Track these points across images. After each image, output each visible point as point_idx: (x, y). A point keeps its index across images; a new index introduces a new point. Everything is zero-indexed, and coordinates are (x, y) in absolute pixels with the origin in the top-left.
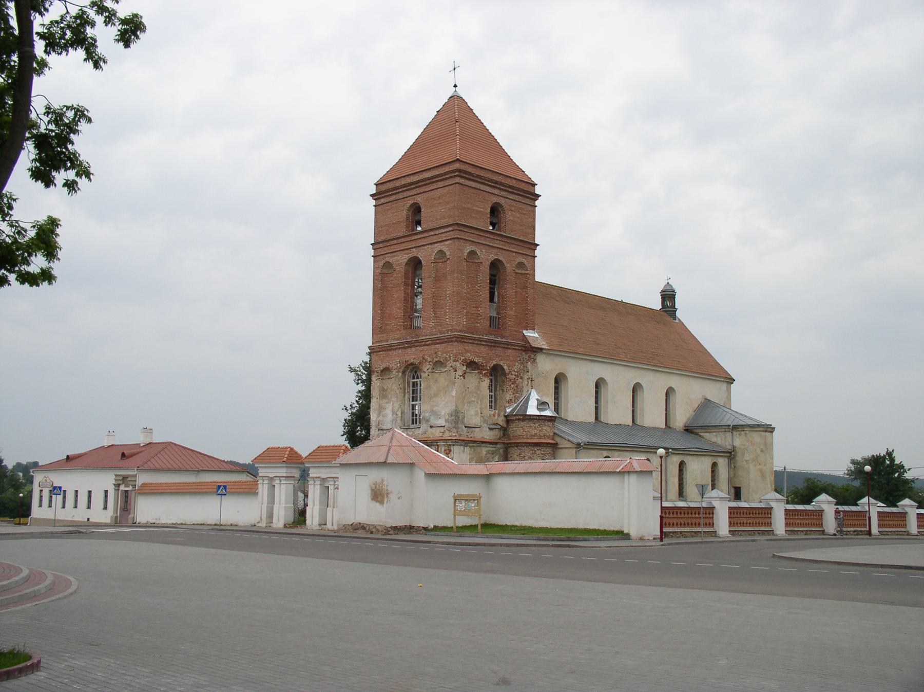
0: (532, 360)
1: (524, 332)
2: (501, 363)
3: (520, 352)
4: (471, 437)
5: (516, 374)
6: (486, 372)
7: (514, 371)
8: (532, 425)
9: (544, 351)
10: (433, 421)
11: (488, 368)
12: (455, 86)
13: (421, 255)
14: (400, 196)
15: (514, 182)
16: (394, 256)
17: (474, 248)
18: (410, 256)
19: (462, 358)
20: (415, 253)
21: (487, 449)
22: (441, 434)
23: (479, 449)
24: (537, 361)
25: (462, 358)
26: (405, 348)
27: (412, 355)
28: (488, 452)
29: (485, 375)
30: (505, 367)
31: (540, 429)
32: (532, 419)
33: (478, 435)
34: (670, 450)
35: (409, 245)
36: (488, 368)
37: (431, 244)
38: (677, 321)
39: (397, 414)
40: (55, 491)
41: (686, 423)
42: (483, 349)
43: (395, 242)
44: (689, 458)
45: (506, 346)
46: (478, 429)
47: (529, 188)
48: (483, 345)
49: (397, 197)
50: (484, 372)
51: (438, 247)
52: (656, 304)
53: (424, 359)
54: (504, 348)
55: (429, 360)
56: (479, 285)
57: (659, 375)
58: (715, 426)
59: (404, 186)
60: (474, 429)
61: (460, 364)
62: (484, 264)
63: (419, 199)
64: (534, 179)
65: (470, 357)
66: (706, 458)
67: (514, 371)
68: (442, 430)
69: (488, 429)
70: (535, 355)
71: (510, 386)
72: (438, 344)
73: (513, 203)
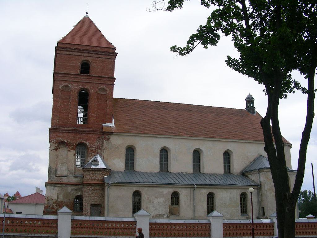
0: (107, 139)
1: (103, 124)
2: (85, 142)
3: (100, 135)
4: (60, 182)
5: (96, 147)
6: (73, 147)
7: (95, 146)
8: (89, 173)
9: (114, 134)
11: (75, 145)
15: (99, 48)
17: (67, 84)
19: (55, 140)
21: (72, 188)
23: (66, 188)
24: (111, 139)
25: (55, 140)
28: (72, 190)
29: (72, 149)
30: (88, 144)
31: (92, 176)
32: (89, 170)
33: (65, 180)
34: (195, 186)
36: (75, 145)
38: (255, 114)
41: (243, 170)
42: (70, 135)
44: (217, 190)
45: (67, 131)
46: (65, 177)
47: (111, 51)
48: (71, 133)
50: (71, 147)
52: (243, 106)
54: (86, 133)
56: (70, 102)
57: (216, 143)
58: (252, 170)
60: (62, 177)
61: (53, 143)
62: (74, 91)
64: (115, 46)
65: (60, 139)
66: (235, 190)
67: (95, 146)
69: (73, 177)
70: (109, 137)
71: (91, 154)
73: (98, 59)
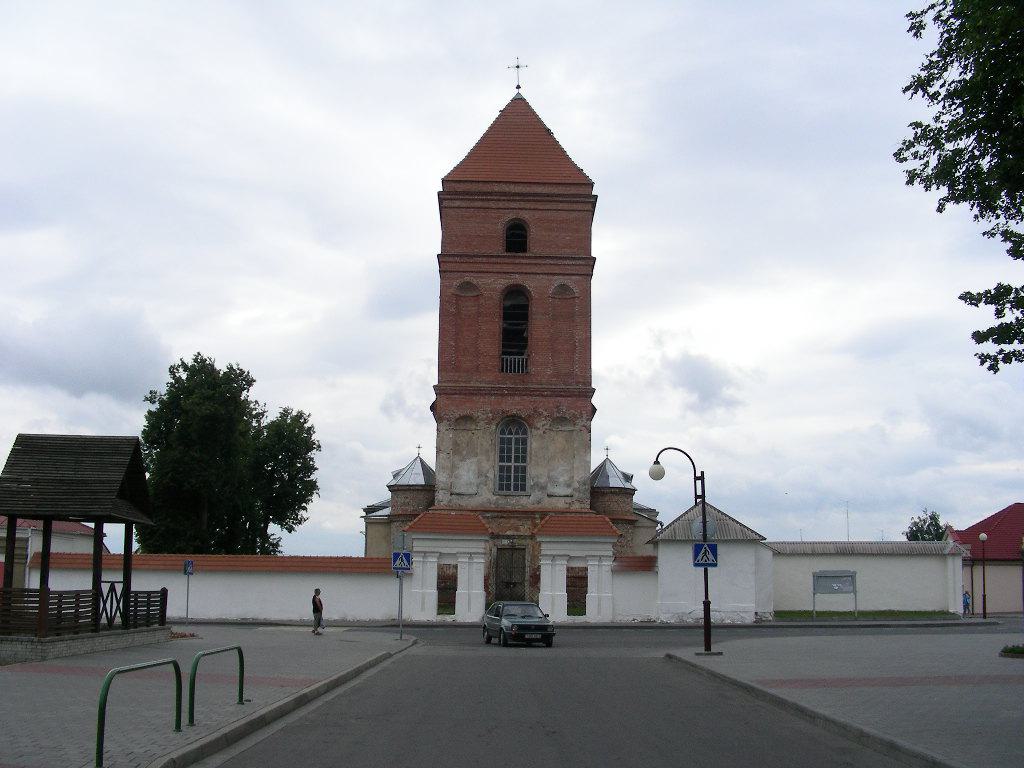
10: (552, 490)
12: (518, 87)
13: (530, 284)
14: (492, 204)
16: (482, 278)
18: (511, 282)
20: (518, 279)
22: (567, 506)
26: (503, 395)
27: (513, 405)
35: (510, 268)
37: (548, 274)
39: (486, 476)
40: (398, 562)
43: (484, 260)
49: (486, 204)
51: (558, 280)
53: (535, 411)
55: (545, 413)
59: (504, 194)
63: (525, 215)
68: (568, 500)
72: (561, 396)
